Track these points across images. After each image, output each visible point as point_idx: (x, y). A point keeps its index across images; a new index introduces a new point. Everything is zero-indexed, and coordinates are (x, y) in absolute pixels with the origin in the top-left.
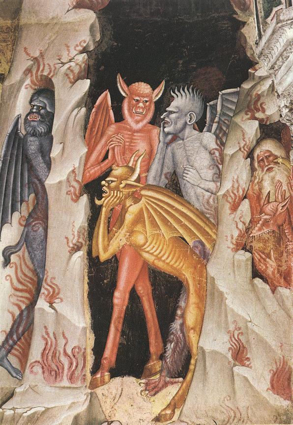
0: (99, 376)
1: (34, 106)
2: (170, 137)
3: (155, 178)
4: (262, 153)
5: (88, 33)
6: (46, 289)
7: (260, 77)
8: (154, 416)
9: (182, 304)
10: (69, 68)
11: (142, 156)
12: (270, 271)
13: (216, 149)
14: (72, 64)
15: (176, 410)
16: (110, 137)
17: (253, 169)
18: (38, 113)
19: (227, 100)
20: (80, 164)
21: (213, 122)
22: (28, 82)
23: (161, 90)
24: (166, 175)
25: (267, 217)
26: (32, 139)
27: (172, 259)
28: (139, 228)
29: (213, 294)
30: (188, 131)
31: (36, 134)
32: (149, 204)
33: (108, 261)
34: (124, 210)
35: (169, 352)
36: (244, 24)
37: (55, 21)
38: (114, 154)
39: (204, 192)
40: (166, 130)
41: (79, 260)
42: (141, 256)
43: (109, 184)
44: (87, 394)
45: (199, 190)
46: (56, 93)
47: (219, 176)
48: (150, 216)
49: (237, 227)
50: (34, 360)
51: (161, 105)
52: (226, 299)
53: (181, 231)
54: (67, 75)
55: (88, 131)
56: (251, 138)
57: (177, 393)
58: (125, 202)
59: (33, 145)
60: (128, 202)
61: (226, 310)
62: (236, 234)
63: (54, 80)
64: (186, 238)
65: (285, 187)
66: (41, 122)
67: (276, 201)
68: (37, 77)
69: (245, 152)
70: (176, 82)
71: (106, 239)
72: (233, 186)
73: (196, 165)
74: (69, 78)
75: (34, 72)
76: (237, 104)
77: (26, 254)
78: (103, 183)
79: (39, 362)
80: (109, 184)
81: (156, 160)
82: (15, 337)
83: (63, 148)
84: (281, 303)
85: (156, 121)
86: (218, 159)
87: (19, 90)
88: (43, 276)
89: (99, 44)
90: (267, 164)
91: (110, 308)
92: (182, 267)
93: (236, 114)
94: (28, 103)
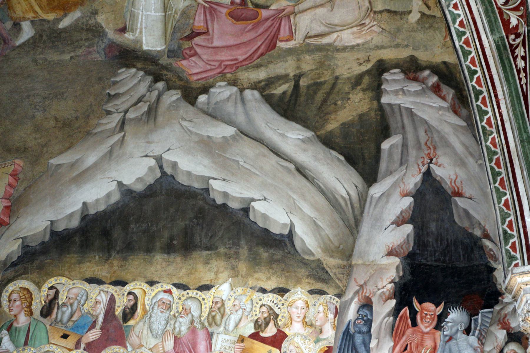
1: (360, 314)
2: (447, 338)
4: (509, 351)
5: (395, 271)
7: (506, 303)
10: (382, 292)
13: (478, 347)
14: (385, 290)
18: (363, 319)
19: (485, 316)
21: (476, 330)
22: (356, 299)
26: (357, 335)
30: (459, 334)
36: (495, 269)
37: (374, 263)
40: (445, 333)
51: (441, 318)
54: (381, 296)
59: (359, 339)
63: (374, 300)
66: (364, 325)
68: (362, 297)
70: (450, 304)
74: (383, 298)
75: (360, 293)
76: (492, 319)
83: (378, 342)
85: (438, 327)
87: (350, 304)
89: (401, 278)
93: (491, 325)
94: (356, 312)
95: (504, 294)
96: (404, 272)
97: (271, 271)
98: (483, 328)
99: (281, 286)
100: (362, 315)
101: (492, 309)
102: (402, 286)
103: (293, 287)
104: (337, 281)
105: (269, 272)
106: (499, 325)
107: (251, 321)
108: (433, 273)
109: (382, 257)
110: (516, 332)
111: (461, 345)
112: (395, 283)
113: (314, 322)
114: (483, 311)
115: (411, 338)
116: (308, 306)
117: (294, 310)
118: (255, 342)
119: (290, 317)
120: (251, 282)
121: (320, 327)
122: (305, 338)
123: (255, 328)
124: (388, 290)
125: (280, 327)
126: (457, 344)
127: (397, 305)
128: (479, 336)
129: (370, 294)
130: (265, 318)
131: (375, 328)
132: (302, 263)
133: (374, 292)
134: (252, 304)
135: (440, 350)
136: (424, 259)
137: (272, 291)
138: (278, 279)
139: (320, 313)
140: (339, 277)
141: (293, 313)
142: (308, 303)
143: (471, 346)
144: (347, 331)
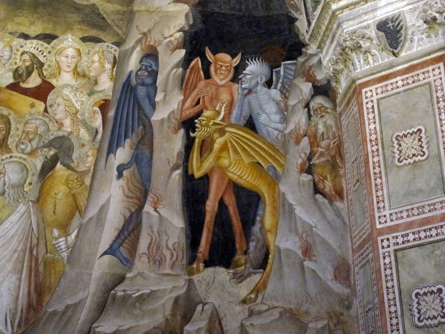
0: (195, 266)
1: (143, 65)
2: (246, 91)
3: (236, 119)
5: (183, 18)
6: (152, 197)
7: (311, 54)
8: (242, 298)
9: (260, 212)
10: (169, 41)
12: (327, 190)
13: (282, 101)
14: (172, 39)
15: (259, 295)
16: (201, 89)
17: (310, 116)
18: (146, 70)
19: (288, 68)
22: (138, 49)
24: (244, 117)
25: (322, 150)
26: (140, 88)
27: (252, 178)
28: (224, 154)
29: (284, 205)
30: (259, 88)
31: (144, 84)
33: (201, 178)
34: (213, 142)
36: (296, 19)
37: (159, 10)
38: (204, 101)
41: (178, 177)
42: (227, 175)
43: (201, 122)
45: (270, 129)
47: (285, 120)
48: (233, 146)
49: (300, 156)
50: (142, 252)
55: (184, 84)
56: (307, 94)
57: (259, 282)
58: (213, 136)
59: (142, 92)
60: (216, 135)
61: (295, 217)
62: (300, 161)
63: (159, 49)
64: (261, 163)
65: (334, 129)
67: (328, 139)
68: (145, 46)
71: (199, 162)
72: (295, 127)
73: (267, 111)
74: (170, 47)
75: (143, 42)
77: (136, 170)
78: (196, 121)
79: (146, 254)
80: (201, 122)
81: (237, 107)
82: (126, 233)
83: (165, 96)
84: (338, 213)
85: (235, 79)
87: (131, 53)
88: (149, 186)
89: (191, 26)
90: (320, 112)
91: (202, 214)
92: (259, 184)
93: (295, 77)
96: (194, 20)
97: (35, 15)
98: (285, 80)
99: (48, 32)
100: (146, 66)
101: (295, 61)
103: (63, 34)
104: (115, 28)
105: (33, 17)
107: (10, 70)
109: (169, 4)
110: (322, 84)
112: (184, 32)
113: (87, 73)
114: (285, 62)
118: (15, 93)
119: (59, 66)
120: (10, 27)
121: (95, 79)
123: (14, 78)
125: (45, 77)
126: (258, 98)
128: (282, 89)
130: (27, 68)
132: (74, 7)
133: (159, 41)
134: (12, 51)
135: (238, 103)
136: (217, 7)
137: (37, 37)
138: (44, 24)
139: (95, 62)
140: (118, 24)
142: (80, 52)
143: (274, 100)
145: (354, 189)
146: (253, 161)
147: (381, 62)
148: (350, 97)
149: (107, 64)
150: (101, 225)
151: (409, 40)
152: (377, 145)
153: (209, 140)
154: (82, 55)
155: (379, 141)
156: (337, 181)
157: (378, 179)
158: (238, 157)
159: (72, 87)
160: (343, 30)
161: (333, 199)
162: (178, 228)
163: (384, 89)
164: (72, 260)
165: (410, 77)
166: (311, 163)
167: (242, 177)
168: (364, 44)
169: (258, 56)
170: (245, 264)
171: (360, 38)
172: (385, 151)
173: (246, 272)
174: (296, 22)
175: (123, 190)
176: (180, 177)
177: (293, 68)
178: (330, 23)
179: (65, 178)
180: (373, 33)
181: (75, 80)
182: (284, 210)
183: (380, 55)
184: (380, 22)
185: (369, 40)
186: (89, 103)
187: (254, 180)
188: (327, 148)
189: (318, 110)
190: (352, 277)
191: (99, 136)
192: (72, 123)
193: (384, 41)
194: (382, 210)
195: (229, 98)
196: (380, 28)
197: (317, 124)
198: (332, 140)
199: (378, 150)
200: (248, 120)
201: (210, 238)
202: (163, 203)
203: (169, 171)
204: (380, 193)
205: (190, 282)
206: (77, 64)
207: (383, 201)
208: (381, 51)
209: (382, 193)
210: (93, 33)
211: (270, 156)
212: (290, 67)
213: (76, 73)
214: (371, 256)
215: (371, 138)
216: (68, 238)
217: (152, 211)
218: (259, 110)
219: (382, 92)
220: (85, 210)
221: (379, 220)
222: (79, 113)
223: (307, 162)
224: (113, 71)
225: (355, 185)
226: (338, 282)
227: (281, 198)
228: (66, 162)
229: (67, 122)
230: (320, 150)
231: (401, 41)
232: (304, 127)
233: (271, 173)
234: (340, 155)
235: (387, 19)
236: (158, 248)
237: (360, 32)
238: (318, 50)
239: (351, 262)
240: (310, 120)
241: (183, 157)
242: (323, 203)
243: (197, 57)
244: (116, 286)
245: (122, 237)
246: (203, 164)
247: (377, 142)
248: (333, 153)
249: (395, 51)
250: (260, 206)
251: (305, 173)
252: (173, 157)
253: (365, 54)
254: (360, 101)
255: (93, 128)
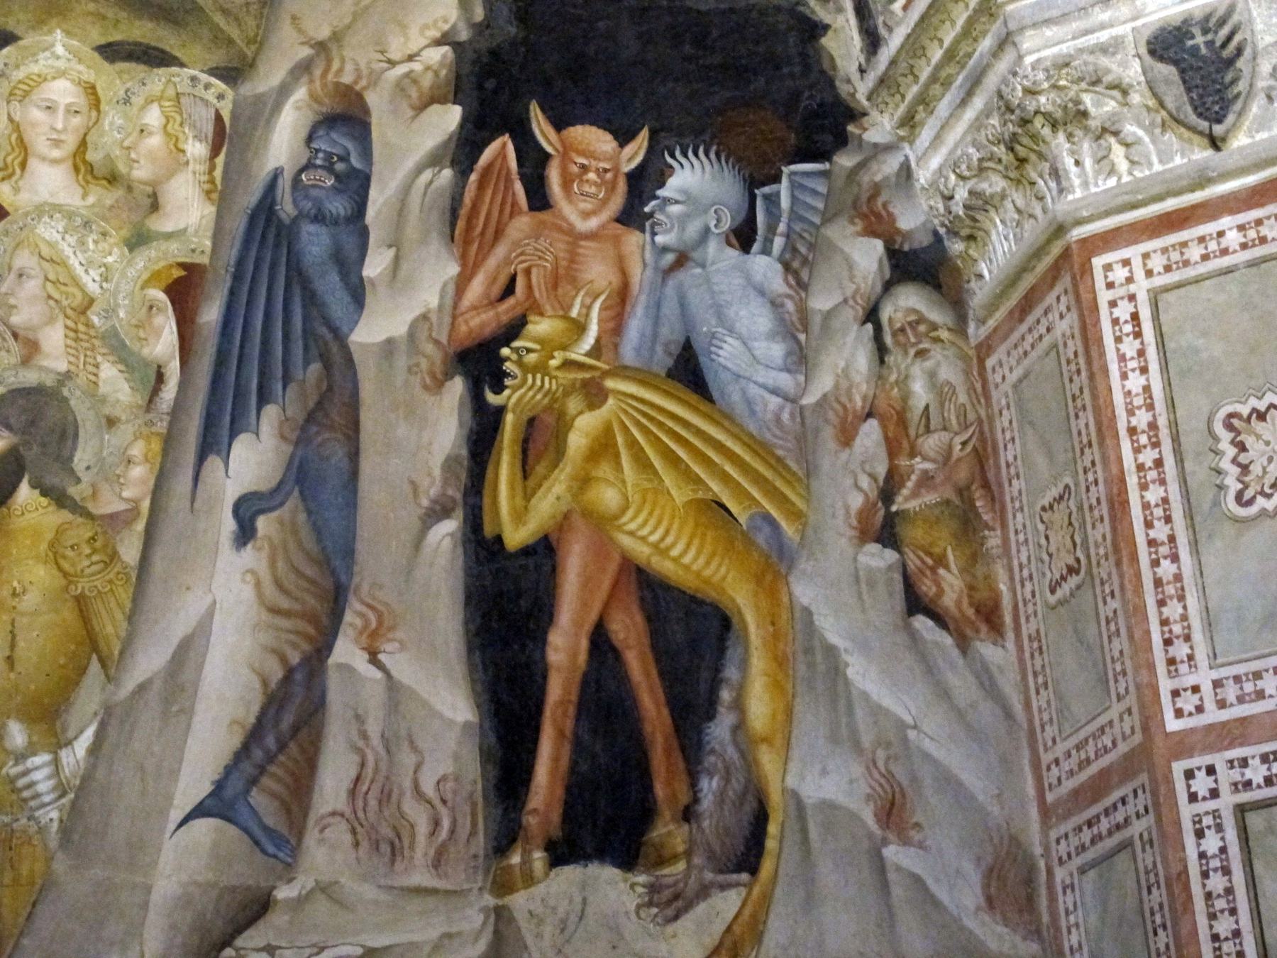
0: (516, 859)
1: (317, 151)
2: (670, 258)
3: (638, 350)
4: (900, 315)
7: (875, 145)
9: (731, 672)
10: (408, 75)
11: (602, 298)
13: (789, 296)
14: (416, 66)
16: (516, 244)
17: (881, 350)
18: (329, 169)
19: (802, 187)
20: (442, 297)
21: (774, 234)
22: (300, 93)
23: (639, 148)
24: (667, 345)
25: (928, 466)
27: (699, 553)
28: (604, 470)
29: (808, 651)
30: (713, 247)
31: (324, 218)
32: (626, 412)
33: (527, 551)
34: (563, 426)
35: (707, 802)
36: (826, 28)
38: (529, 287)
39: (767, 395)
41: (447, 543)
43: (520, 357)
44: (485, 910)
45: (754, 391)
46: (374, 128)
48: (633, 444)
50: (330, 809)
52: (847, 665)
53: (716, 486)
54: (403, 90)
55: (461, 224)
56: (871, 276)
57: (736, 917)
58: (564, 404)
60: (573, 404)
62: (857, 501)
63: (372, 99)
64: (729, 505)
65: (962, 398)
67: (945, 429)
68: (324, 85)
69: (859, 308)
73: (742, 327)
75: (318, 72)
77: (302, 517)
78: (505, 351)
79: (342, 815)
81: (640, 311)
83: (397, 260)
84: (987, 681)
86: (795, 318)
87: (277, 107)
88: (350, 574)
89: (480, 29)
90: (913, 340)
92: (724, 578)
93: (828, 218)
94: (302, 144)
95: (865, 114)
98: (798, 227)
100: (329, 156)
101: (827, 166)
102: (485, 60)
103: (33, 28)
104: (219, 19)
106: (857, 220)
108: (601, 24)
110: (916, 245)
111: (723, 287)
112: (457, 46)
113: (122, 168)
114: (794, 167)
115: (529, 250)
116: (96, 103)
117: (37, 114)
119: (21, 140)
121: (149, 189)
122: (87, 224)
124: (428, 68)
126: (708, 281)
127: (470, 126)
128: (788, 256)
129: (359, 77)
131: (385, 204)
133: (372, 72)
135: (643, 298)
139: (151, 134)
141: (34, 125)
143: (761, 292)
144: (265, 209)
145: (1052, 599)
146: (700, 495)
147: (1158, 167)
148: (1033, 289)
149: (190, 141)
150: (181, 711)
151: (1263, 95)
152: (1156, 445)
153: (550, 420)
154: (103, 107)
155: (1164, 434)
156: (980, 571)
157: (1166, 564)
158: (650, 480)
159: (70, 215)
160: (1020, 57)
161: (969, 632)
162: (451, 723)
163: (1175, 256)
164: (76, 837)
165: (1268, 218)
166: (894, 508)
167: (668, 549)
168: (1098, 104)
169: (704, 141)
170: (688, 854)
171: (1083, 85)
172: (1187, 465)
173: (693, 883)
174: (824, 34)
175: (258, 584)
176: (455, 546)
177: (822, 188)
178: (969, 33)
179: (49, 536)
180: (1133, 71)
181: (80, 190)
182: (811, 665)
183: (1154, 141)
184: (1163, 29)
185: (1115, 93)
186: (131, 272)
187: (708, 563)
188: (940, 459)
189: (909, 331)
190: (1043, 902)
191: (170, 391)
192: (69, 342)
193: (1175, 95)
194: (1183, 668)
195: (615, 280)
196: (1160, 52)
197: (907, 377)
198: (956, 434)
199: (1159, 463)
200: (680, 356)
201: (565, 762)
202: (399, 634)
203: (417, 524)
204: (1173, 610)
205: (501, 915)
206: (85, 135)
207: (1187, 638)
208: (1158, 131)
209: (1180, 611)
210: (141, 31)
211: (758, 479)
212: (811, 183)
213: (83, 169)
214: (1138, 827)
215: (1134, 422)
216: (64, 754)
217: (360, 662)
218: (713, 322)
219: (1168, 269)
220: (122, 653)
221: (1174, 703)
222: (95, 308)
223: (880, 504)
224: (212, 168)
225: (1058, 584)
226: (998, 917)
227: (798, 627)
228: (52, 480)
229: (54, 339)
230: (920, 465)
231: (1239, 94)
232: (864, 387)
233: (761, 539)
234: (986, 485)
235: (1185, 22)
236: (386, 797)
237: (1086, 63)
238: (901, 133)
239: (1038, 850)
240: (882, 361)
241: (464, 476)
242: (936, 643)
243: (503, 134)
244: (239, 931)
245: (258, 754)
246: (533, 501)
247: (1157, 436)
248: (962, 474)
249: (1218, 129)
250: (729, 653)
251: (878, 541)
252: (429, 475)
253: (1098, 138)
254: (1085, 296)
255: (147, 364)
